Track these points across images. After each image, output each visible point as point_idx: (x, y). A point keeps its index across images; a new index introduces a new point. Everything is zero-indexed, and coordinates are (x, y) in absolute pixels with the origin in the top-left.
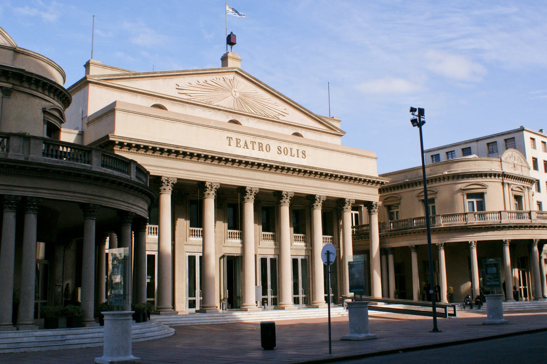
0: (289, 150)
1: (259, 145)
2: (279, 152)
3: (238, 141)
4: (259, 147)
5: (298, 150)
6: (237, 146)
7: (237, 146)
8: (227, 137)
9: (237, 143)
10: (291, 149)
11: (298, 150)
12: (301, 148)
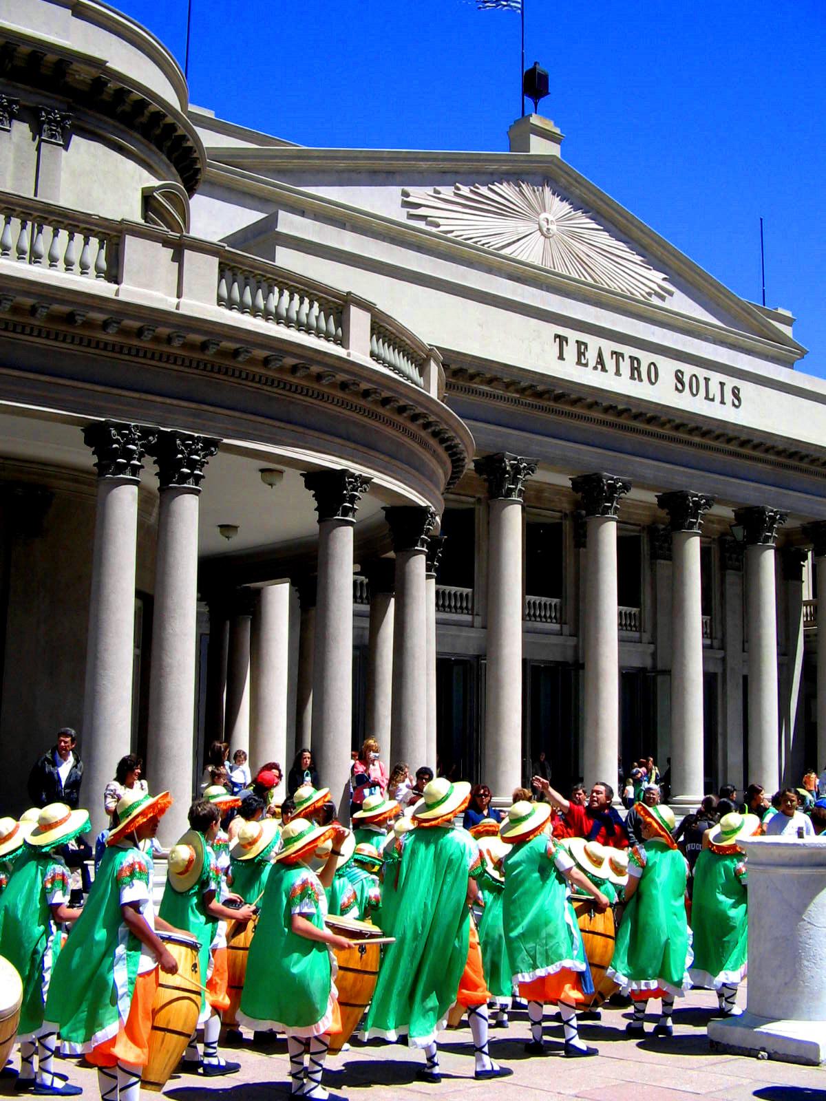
0: (702, 383)
1: (632, 364)
2: (680, 387)
3: (582, 347)
4: (633, 369)
5: (722, 384)
6: (579, 363)
7: (579, 363)
8: (557, 336)
9: (580, 354)
10: (707, 380)
12: (731, 382)
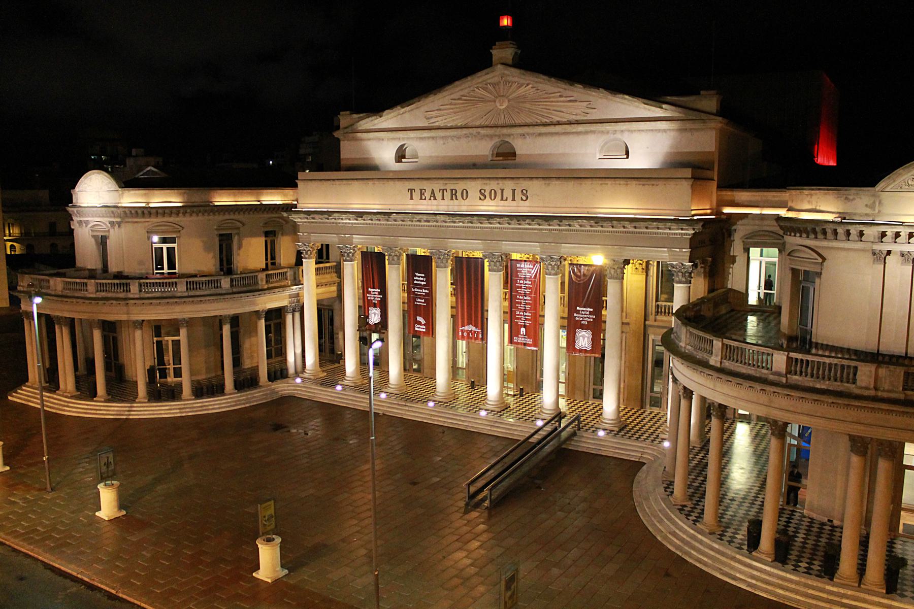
2: (482, 197)
5: (514, 191)
6: (421, 199)
7: (421, 199)
9: (422, 194)
10: (502, 191)
11: (514, 191)
